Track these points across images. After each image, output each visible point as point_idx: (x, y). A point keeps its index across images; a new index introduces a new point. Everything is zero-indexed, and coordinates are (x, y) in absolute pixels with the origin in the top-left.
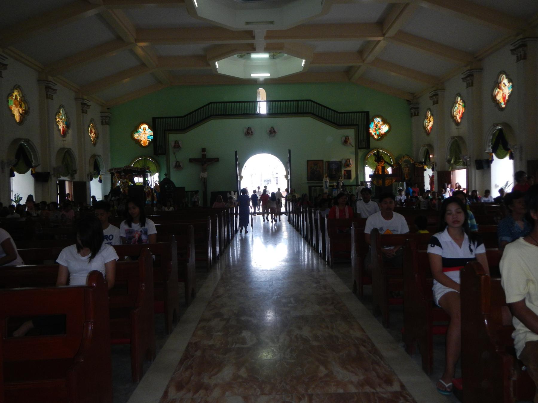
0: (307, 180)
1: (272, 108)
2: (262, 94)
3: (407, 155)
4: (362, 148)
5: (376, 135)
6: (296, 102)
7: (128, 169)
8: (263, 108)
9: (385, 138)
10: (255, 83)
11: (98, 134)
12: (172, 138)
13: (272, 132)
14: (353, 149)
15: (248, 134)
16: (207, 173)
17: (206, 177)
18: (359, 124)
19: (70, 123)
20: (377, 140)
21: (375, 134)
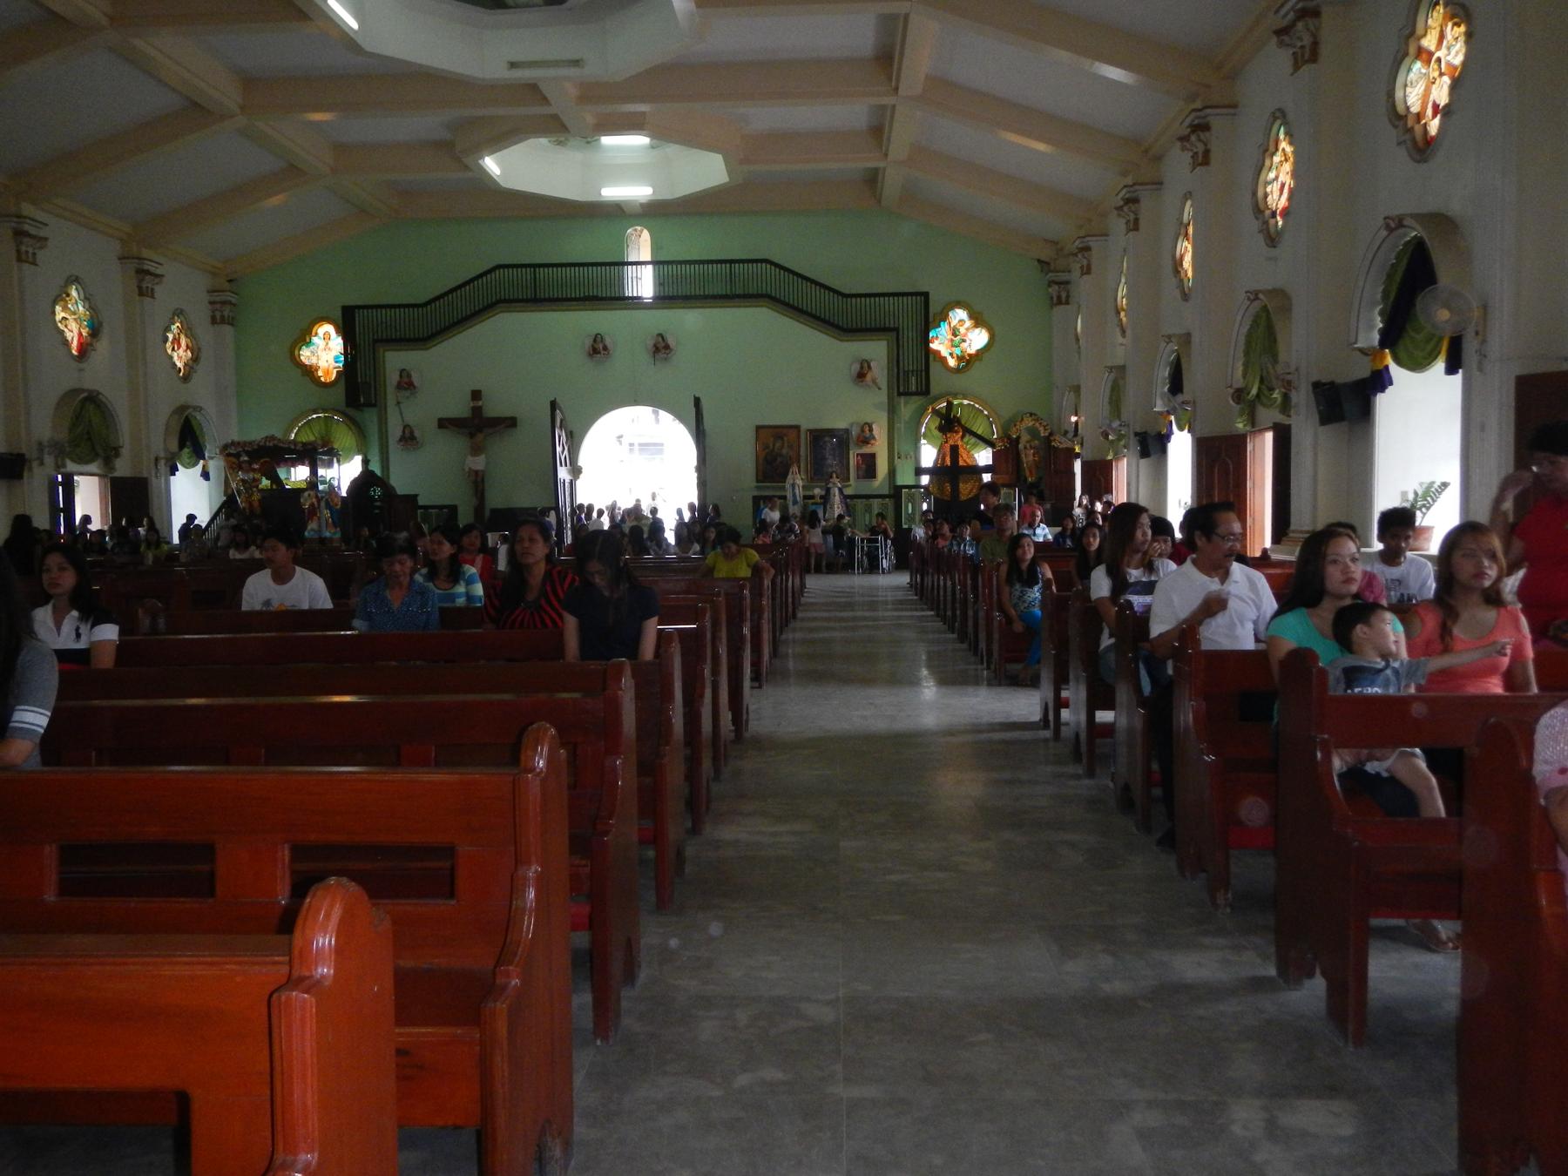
0: (754, 478)
1: (666, 281)
2: (641, 246)
3: (1031, 414)
4: (907, 394)
5: (953, 357)
6: (728, 265)
7: (271, 444)
8: (643, 283)
9: (976, 369)
10: (618, 214)
11: (199, 349)
12: (395, 361)
13: (661, 348)
14: (882, 397)
16: (483, 456)
18: (901, 327)
19: (101, 324)
20: (957, 370)
21: (951, 354)
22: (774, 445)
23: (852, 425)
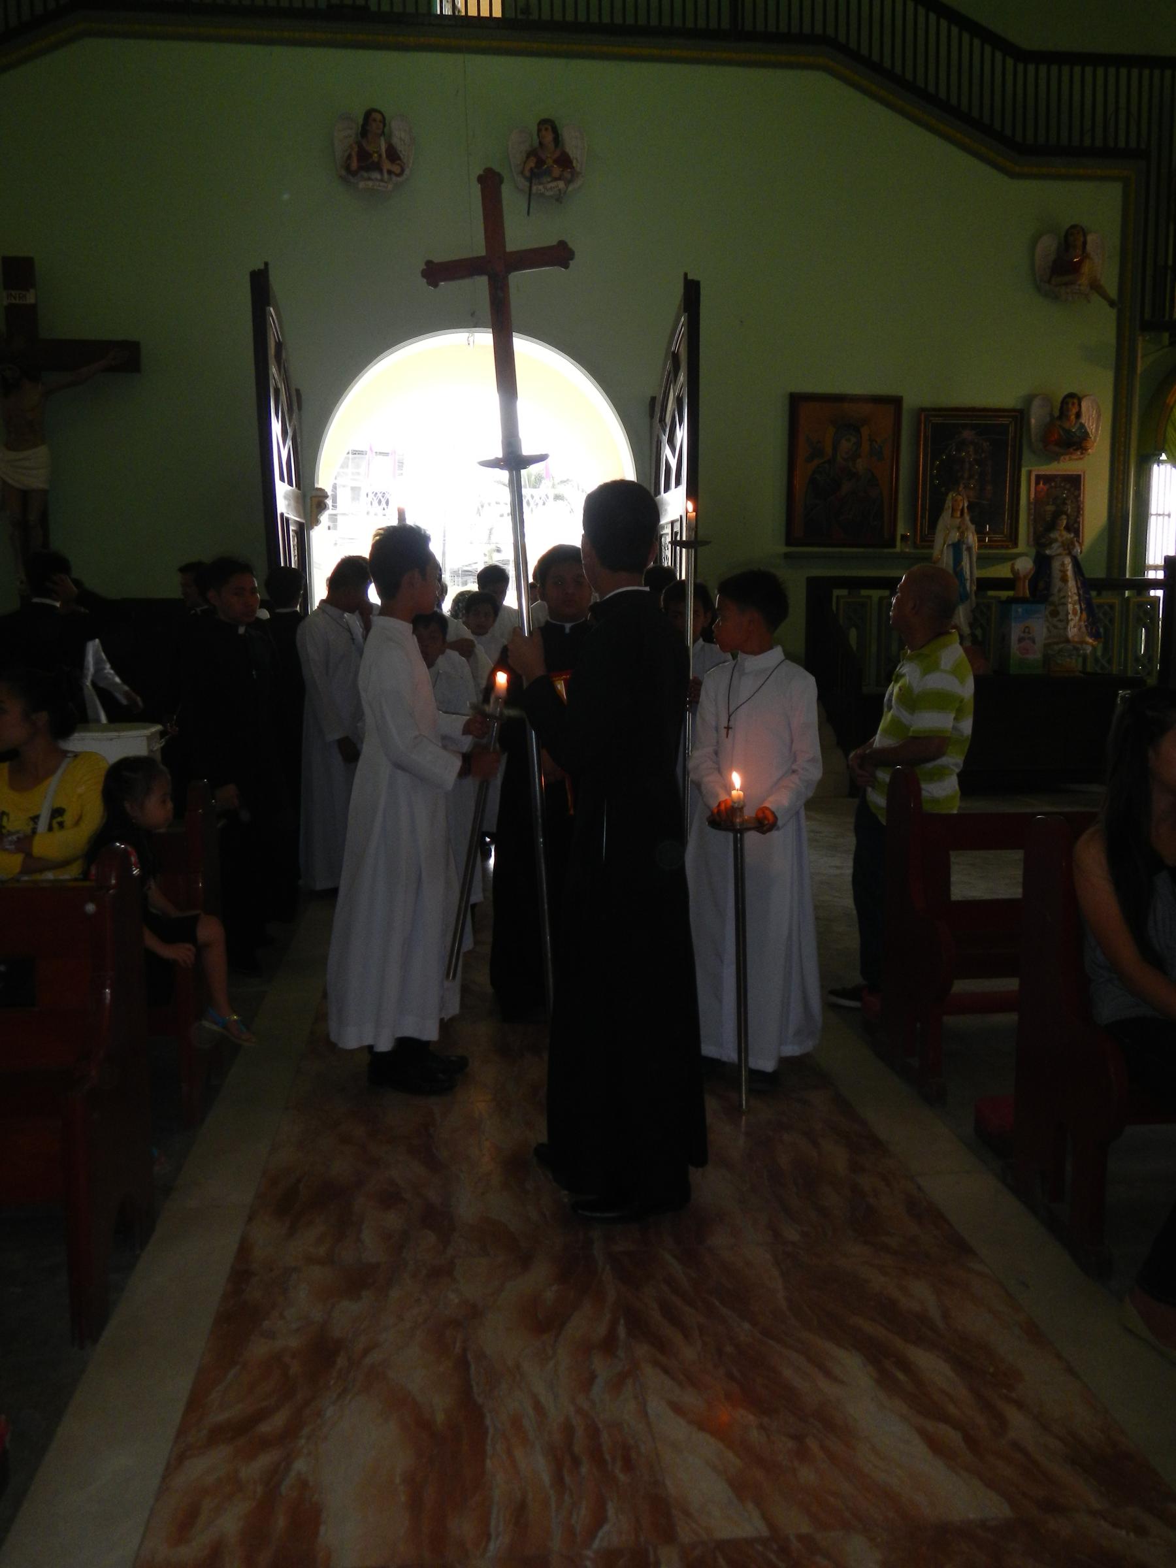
16: (42, 451)
17: (42, 486)
23: (1029, 399)
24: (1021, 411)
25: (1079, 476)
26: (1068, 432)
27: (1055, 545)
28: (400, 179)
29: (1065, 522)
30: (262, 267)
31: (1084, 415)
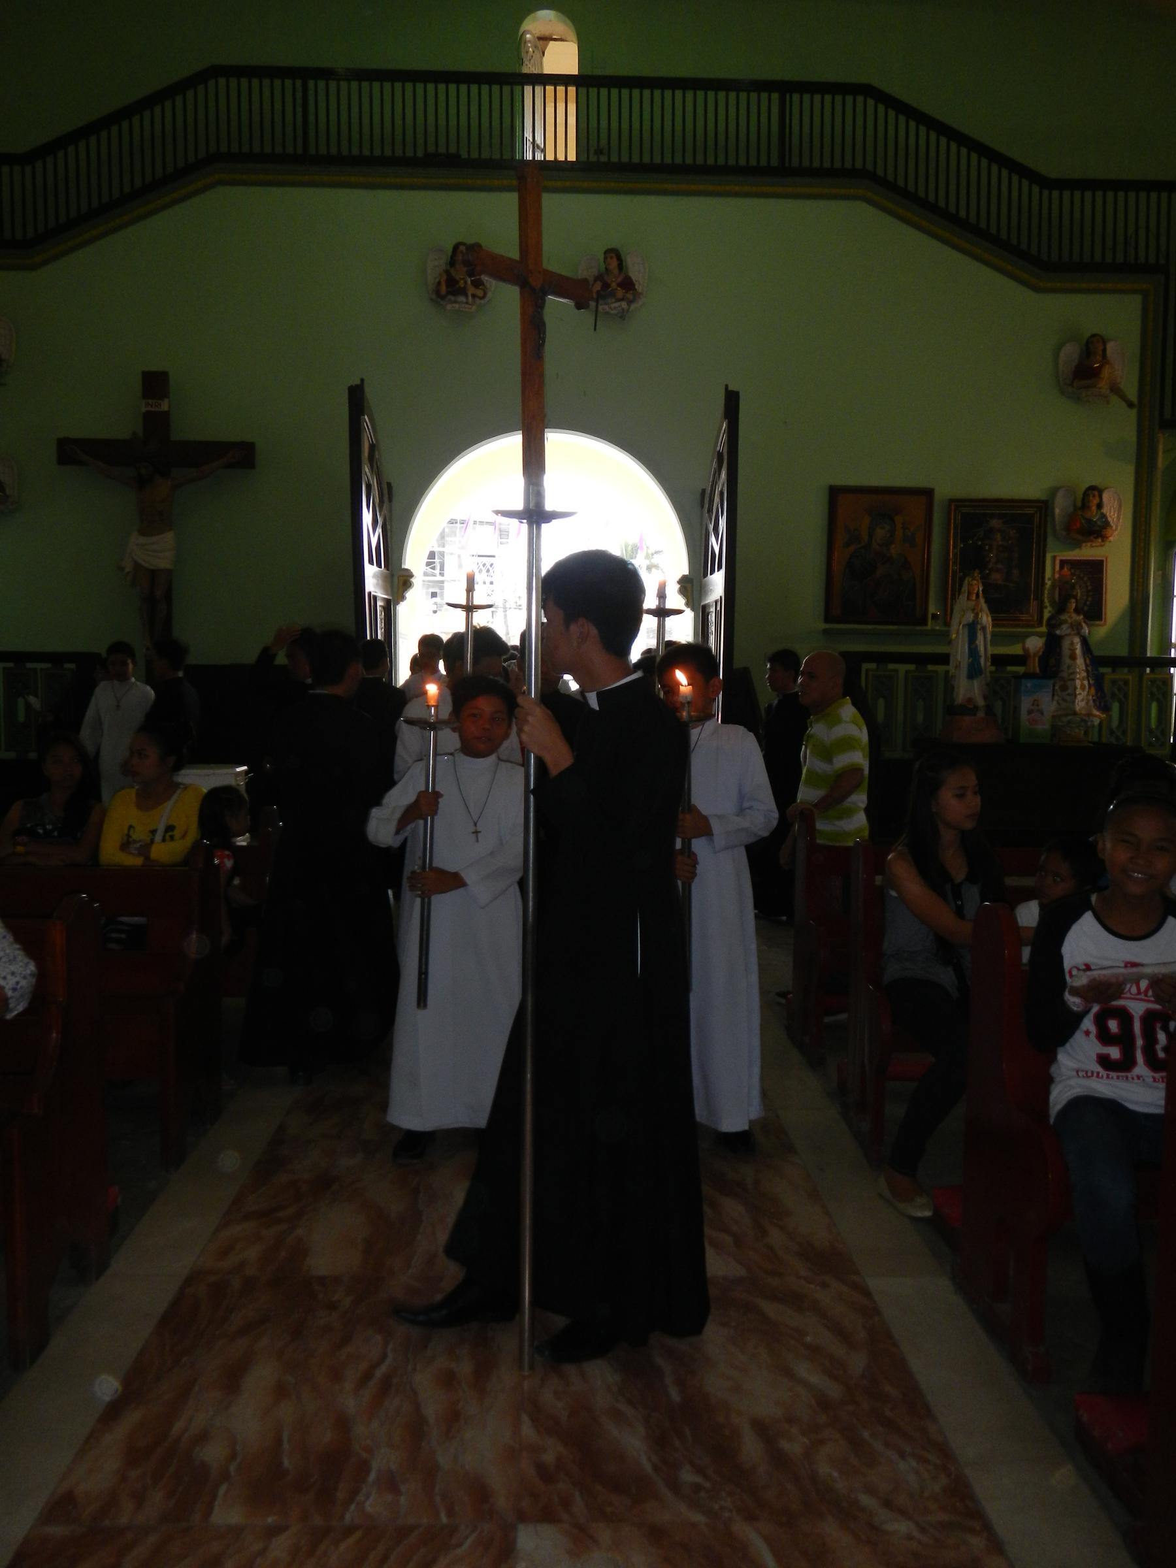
6: (775, 96)
15: (448, 293)
16: (169, 538)
17: (169, 566)
22: (871, 536)
23: (1054, 491)
24: (1045, 502)
25: (1102, 561)
26: (1089, 521)
27: (1065, 627)
28: (482, 302)
29: (1074, 605)
30: (358, 382)
31: (1105, 506)
